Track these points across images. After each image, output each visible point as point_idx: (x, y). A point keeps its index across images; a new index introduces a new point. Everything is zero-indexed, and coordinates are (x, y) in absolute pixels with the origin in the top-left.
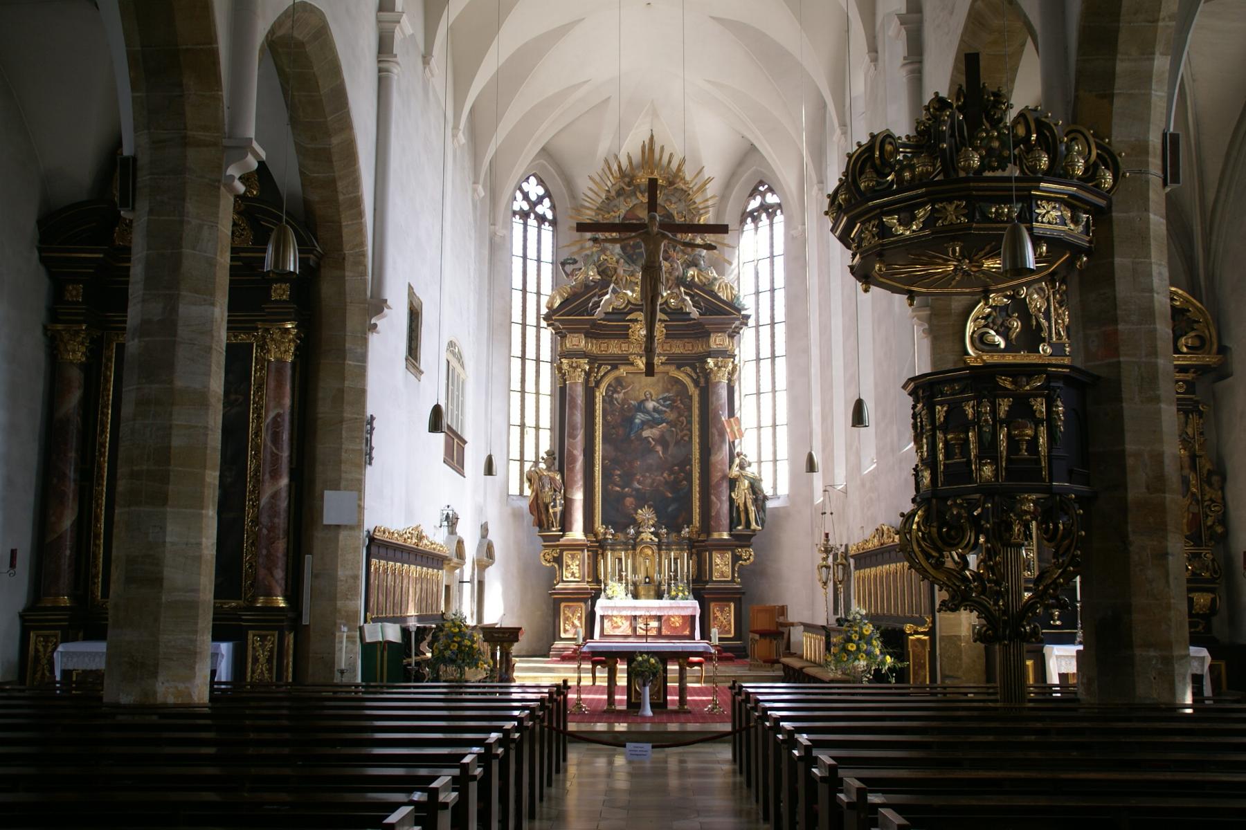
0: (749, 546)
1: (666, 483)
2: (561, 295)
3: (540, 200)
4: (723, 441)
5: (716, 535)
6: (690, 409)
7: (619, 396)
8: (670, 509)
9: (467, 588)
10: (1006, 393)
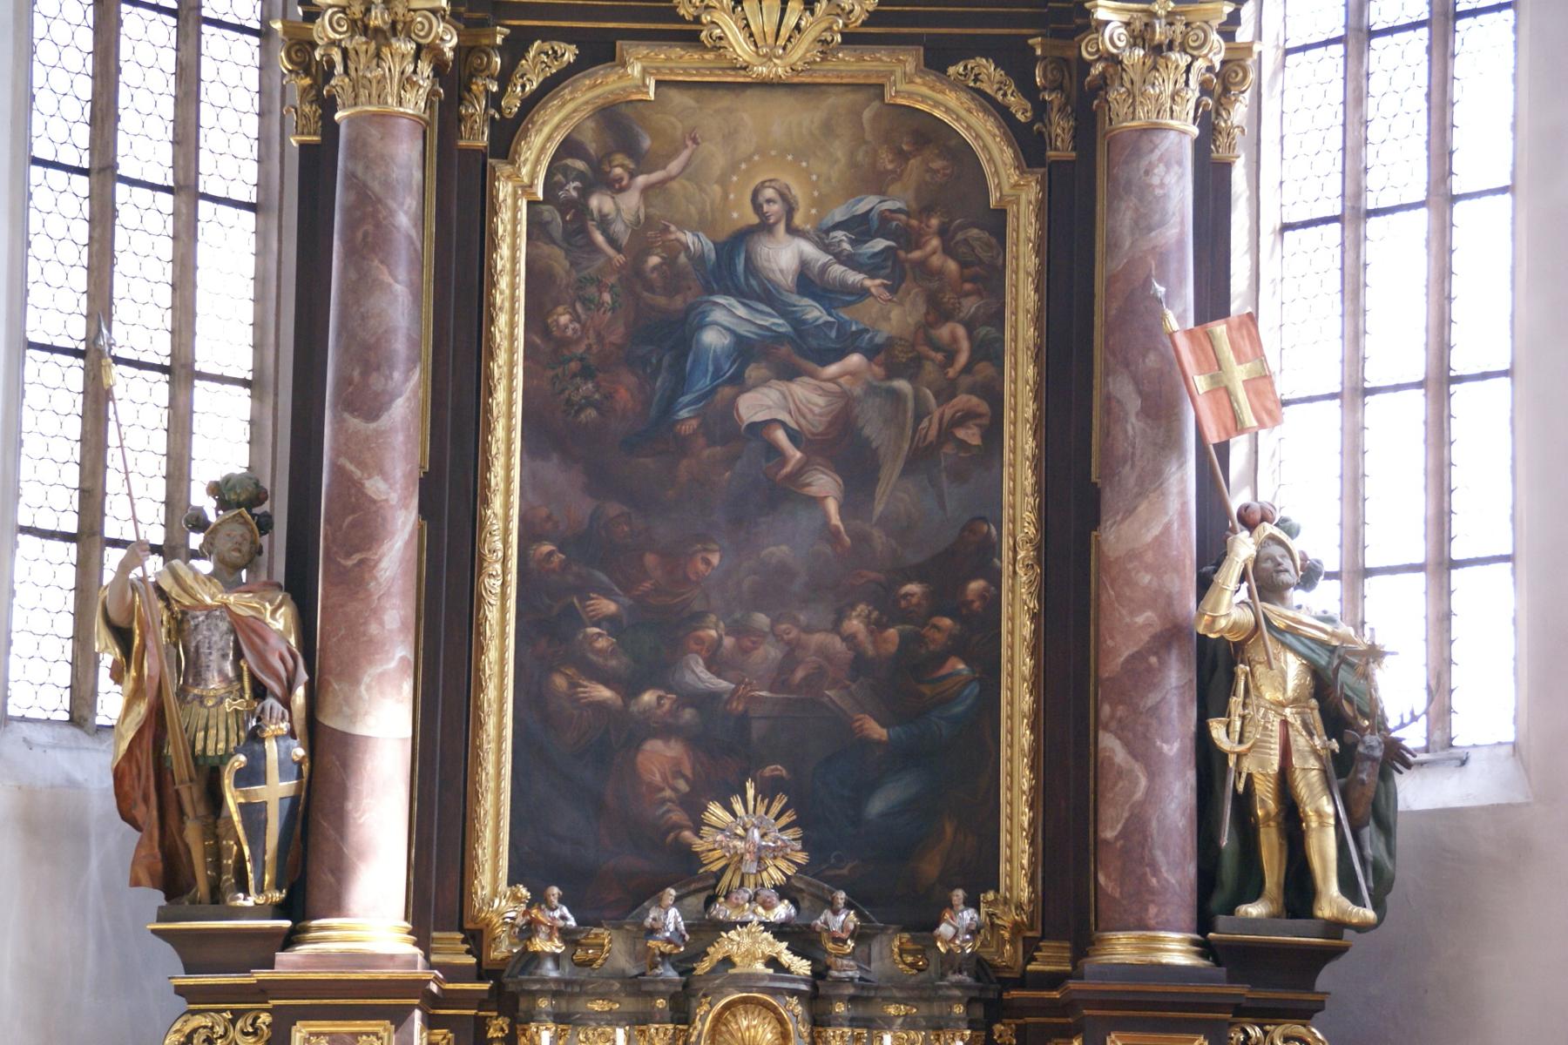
0: (1304, 1014)
1: (859, 664)
4: (1170, 443)
5: (1122, 948)
6: (989, 278)
7: (620, 207)
8: (877, 805)
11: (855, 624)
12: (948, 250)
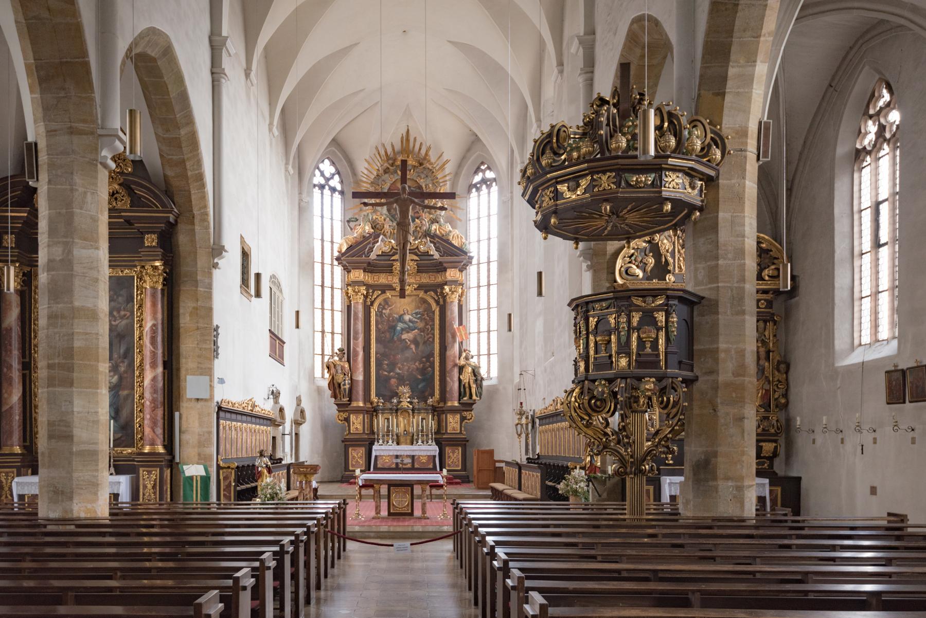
1: (417, 369)
4: (454, 341)
5: (449, 404)
6: (433, 320)
7: (386, 312)
8: (420, 386)
9: (287, 438)
10: (638, 309)
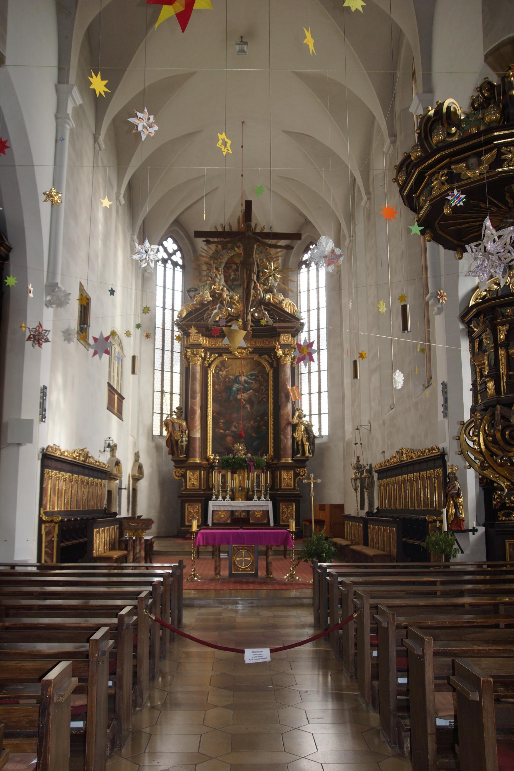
0: (304, 467)
2: (187, 310)
3: (175, 252)
5: (283, 461)
6: (267, 381)
7: (223, 373)
8: (255, 444)
9: (124, 493)
11: (252, 423)
12: (262, 378)
